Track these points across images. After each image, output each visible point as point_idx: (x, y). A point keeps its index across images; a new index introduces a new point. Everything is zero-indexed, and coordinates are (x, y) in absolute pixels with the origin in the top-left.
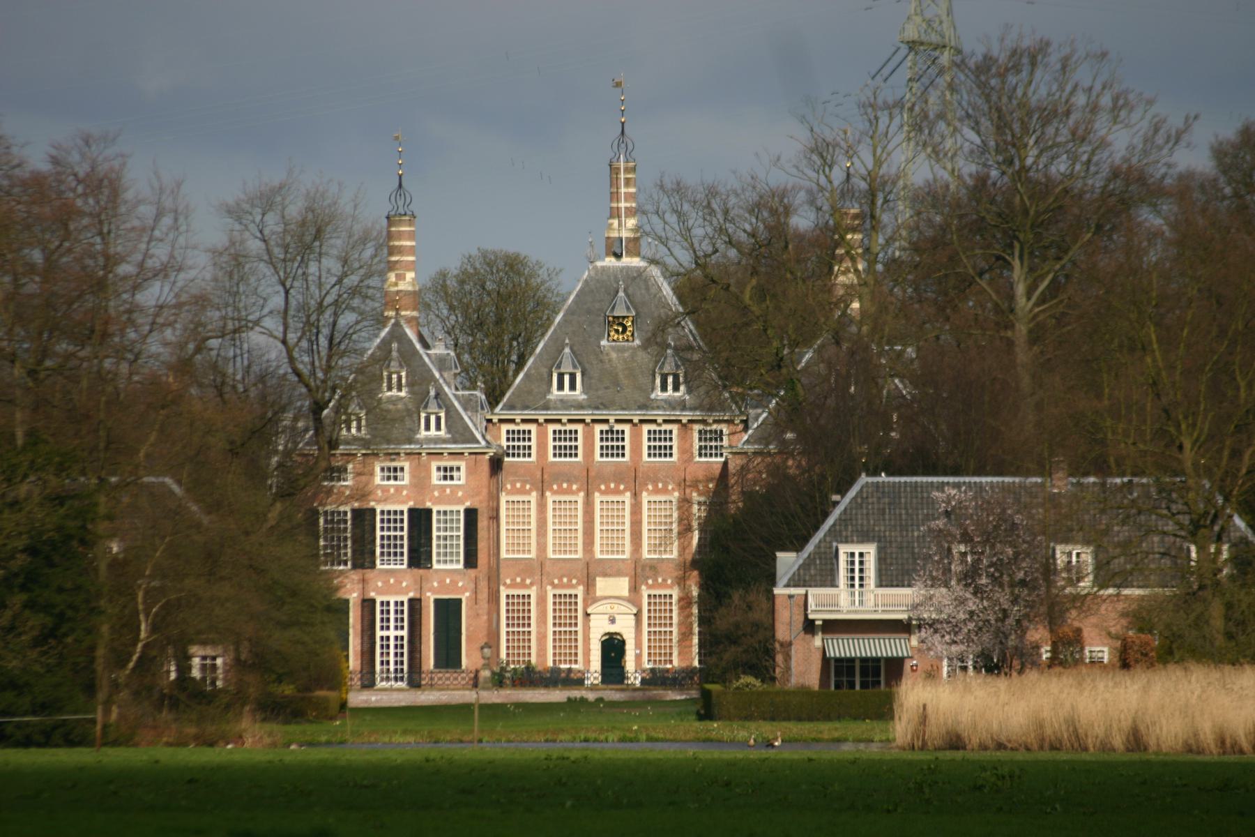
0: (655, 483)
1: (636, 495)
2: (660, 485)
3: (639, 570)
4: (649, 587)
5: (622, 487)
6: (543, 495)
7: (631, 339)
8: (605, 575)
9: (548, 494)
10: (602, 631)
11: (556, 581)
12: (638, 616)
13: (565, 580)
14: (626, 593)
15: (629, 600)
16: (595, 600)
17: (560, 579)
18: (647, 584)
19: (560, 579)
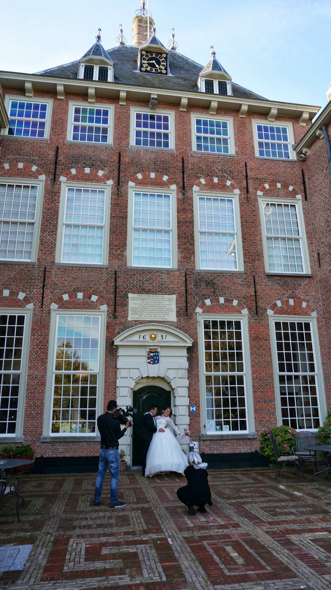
0: (209, 175)
1: (184, 189)
2: (216, 180)
3: (191, 286)
4: (207, 310)
5: (165, 178)
6: (55, 179)
7: (164, 72)
8: (142, 290)
9: (63, 179)
10: (136, 375)
11: (66, 297)
12: (192, 351)
13: (80, 295)
14: (173, 317)
15: (178, 326)
16: (126, 326)
17: (73, 295)
18: (203, 305)
19: (73, 295)
